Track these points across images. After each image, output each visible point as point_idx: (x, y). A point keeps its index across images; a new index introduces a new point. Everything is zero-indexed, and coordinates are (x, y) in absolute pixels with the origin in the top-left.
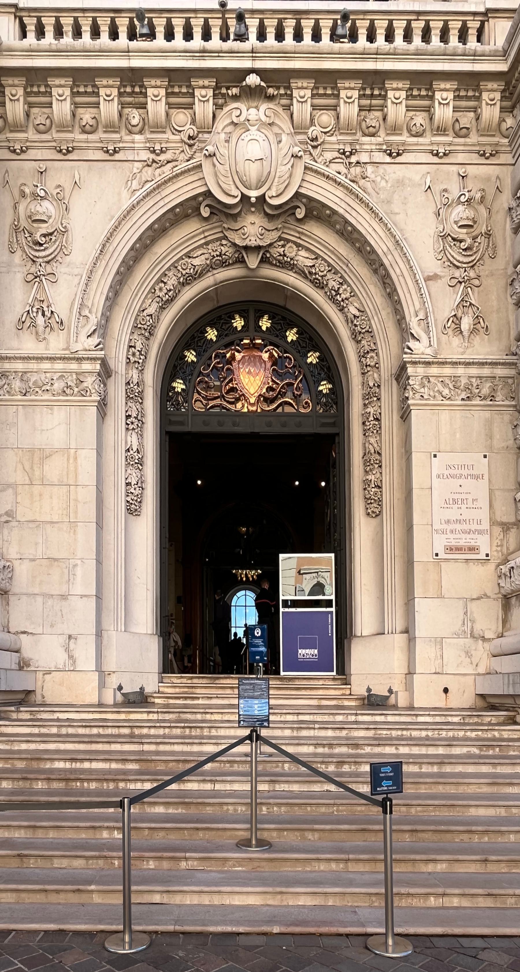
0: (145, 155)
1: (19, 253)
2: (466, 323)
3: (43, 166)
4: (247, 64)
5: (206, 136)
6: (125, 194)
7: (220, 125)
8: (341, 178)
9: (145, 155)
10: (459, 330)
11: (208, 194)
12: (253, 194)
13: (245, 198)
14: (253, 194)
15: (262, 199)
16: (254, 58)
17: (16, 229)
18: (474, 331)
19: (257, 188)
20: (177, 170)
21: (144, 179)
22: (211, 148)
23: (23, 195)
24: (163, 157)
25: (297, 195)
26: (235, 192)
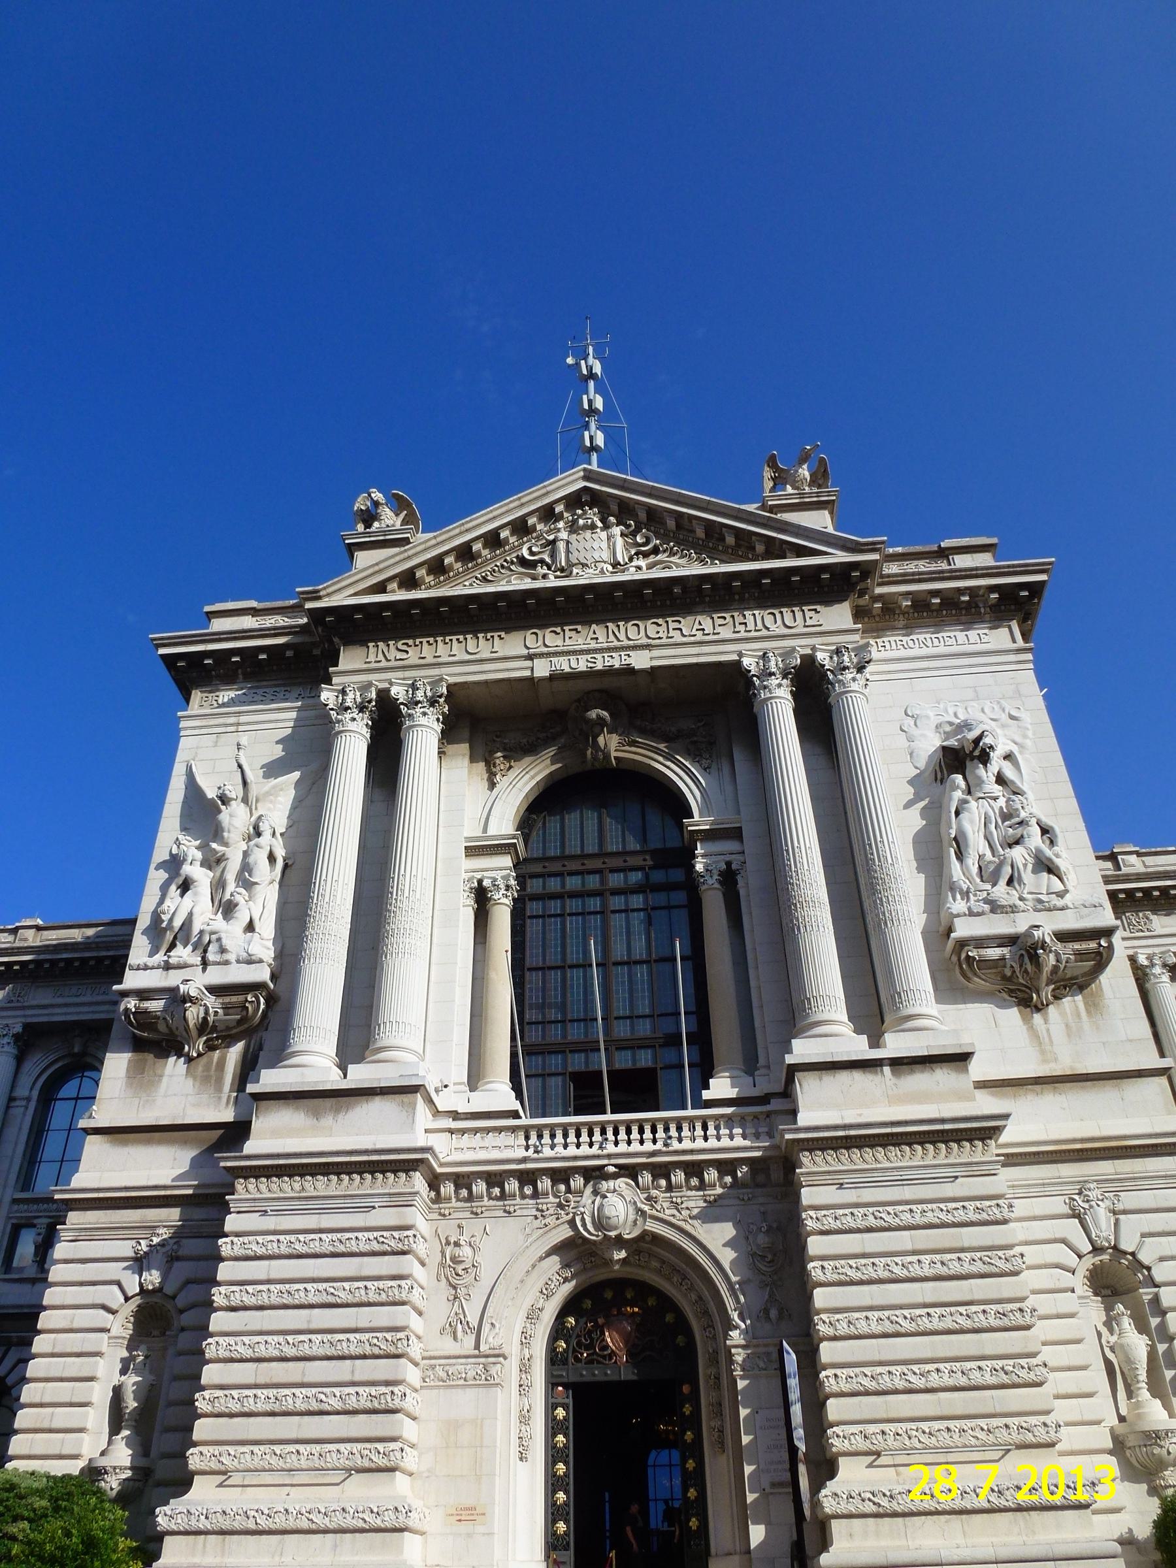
1: (444, 1280)
2: (773, 1313)
4: (605, 1162)
6: (521, 1237)
9: (534, 1212)
10: (768, 1318)
15: (619, 1237)
16: (609, 1159)
17: (442, 1265)
18: (780, 1317)
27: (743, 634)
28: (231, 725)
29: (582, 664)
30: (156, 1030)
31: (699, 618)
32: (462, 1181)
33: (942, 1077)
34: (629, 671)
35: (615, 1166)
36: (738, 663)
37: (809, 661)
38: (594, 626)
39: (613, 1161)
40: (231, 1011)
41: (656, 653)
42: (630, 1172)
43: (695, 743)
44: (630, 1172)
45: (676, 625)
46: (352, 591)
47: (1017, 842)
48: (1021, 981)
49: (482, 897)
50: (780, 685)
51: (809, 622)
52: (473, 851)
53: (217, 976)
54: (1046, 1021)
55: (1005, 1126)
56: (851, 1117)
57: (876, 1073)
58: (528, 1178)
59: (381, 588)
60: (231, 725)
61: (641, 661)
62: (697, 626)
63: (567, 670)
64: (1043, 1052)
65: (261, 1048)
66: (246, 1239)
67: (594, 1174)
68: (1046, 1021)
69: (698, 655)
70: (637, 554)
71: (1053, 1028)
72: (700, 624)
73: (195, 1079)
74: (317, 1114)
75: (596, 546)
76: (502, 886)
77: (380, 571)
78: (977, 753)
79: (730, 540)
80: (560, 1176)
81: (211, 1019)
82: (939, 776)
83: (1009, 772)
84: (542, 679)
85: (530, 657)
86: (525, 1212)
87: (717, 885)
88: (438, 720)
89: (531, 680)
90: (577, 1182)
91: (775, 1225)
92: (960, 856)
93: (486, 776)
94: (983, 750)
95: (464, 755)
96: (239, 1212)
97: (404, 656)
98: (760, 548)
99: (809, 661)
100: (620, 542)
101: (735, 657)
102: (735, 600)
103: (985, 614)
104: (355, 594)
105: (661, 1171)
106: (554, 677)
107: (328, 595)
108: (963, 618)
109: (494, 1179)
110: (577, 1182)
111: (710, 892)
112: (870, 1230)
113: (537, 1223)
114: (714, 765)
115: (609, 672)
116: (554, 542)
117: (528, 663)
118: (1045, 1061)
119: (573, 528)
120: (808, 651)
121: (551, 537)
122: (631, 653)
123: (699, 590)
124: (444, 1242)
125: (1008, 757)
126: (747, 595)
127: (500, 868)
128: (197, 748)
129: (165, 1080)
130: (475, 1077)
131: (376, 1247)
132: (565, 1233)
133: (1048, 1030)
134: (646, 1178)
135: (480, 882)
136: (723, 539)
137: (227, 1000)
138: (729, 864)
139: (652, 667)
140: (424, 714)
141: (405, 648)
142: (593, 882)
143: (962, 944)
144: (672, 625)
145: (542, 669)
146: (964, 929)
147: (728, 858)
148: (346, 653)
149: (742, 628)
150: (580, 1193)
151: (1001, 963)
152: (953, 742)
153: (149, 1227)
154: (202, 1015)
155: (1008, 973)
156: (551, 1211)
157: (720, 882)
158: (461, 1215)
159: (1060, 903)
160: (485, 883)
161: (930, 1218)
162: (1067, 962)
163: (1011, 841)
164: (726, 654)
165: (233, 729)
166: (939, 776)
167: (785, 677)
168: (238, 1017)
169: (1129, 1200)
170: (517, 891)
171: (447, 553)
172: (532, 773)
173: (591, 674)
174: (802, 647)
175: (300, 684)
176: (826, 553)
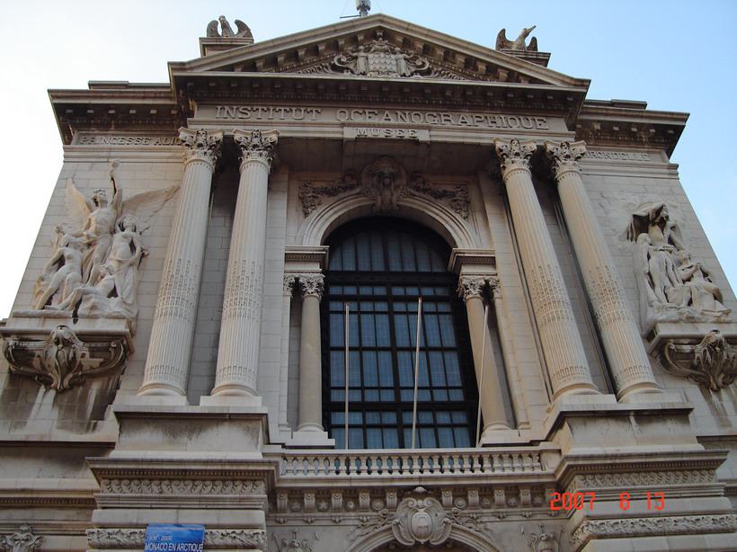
0: (357, 522)
3: (297, 529)
5: (393, 513)
7: (400, 508)
8: (472, 531)
9: (357, 522)
11: (396, 540)
12: (422, 541)
13: (418, 544)
14: (422, 541)
19: (424, 538)
20: (377, 531)
21: (357, 534)
22: (397, 520)
23: (285, 545)
24: (368, 524)
25: (449, 539)
26: (412, 540)
27: (494, 128)
28: (104, 157)
29: (381, 134)
30: (31, 366)
31: (462, 115)
32: (297, 494)
33: (670, 428)
34: (415, 142)
36: (493, 146)
37: (541, 150)
38: (387, 112)
39: (422, 483)
40: (97, 354)
41: (433, 133)
42: (434, 492)
43: (455, 201)
44: (434, 492)
45: (447, 118)
46: (209, 68)
47: (689, 280)
48: (703, 369)
49: (297, 289)
51: (539, 127)
52: (290, 258)
53: (83, 326)
54: (720, 399)
55: (725, 460)
56: (611, 450)
57: (625, 421)
58: (351, 494)
59: (231, 68)
60: (104, 157)
61: (423, 136)
62: (461, 120)
63: (370, 136)
64: (721, 420)
65: (118, 388)
66: (110, 530)
67: (404, 492)
68: (720, 399)
69: (463, 137)
70: (416, 72)
71: (724, 403)
72: (463, 118)
73: (61, 407)
74: (174, 434)
75: (388, 62)
76: (315, 284)
78: (657, 221)
79: (482, 67)
80: (378, 493)
81: (79, 359)
82: (630, 236)
83: (676, 239)
84: (349, 141)
85: (343, 125)
86: (348, 522)
87: (478, 296)
89: (341, 141)
90: (392, 499)
91: (551, 536)
92: (652, 285)
93: (301, 208)
94: (662, 218)
95: (284, 192)
96: (104, 508)
97: (245, 116)
98: (503, 74)
99: (541, 150)
100: (403, 63)
101: (491, 142)
102: (487, 107)
105: (460, 491)
106: (358, 140)
107: (192, 69)
109: (323, 494)
110: (392, 499)
111: (474, 300)
112: (636, 535)
113: (358, 532)
114: (470, 216)
116: (356, 58)
117: (339, 129)
118: (724, 426)
119: (368, 50)
120: (542, 144)
121: (355, 54)
123: (464, 95)
124: (279, 543)
125: (673, 228)
127: (312, 273)
128: (76, 170)
129: (35, 408)
130: (295, 422)
131: (229, 541)
132: (383, 540)
133: (722, 405)
134: (447, 498)
135: (297, 279)
136: (476, 69)
137: (93, 345)
138: (487, 282)
139: (431, 142)
140: (261, 155)
141: (246, 111)
142: (380, 291)
143: (664, 340)
144: (443, 118)
145: (350, 133)
146: (663, 331)
147: (487, 278)
148: (200, 111)
149: (494, 125)
150: (394, 508)
151: (692, 356)
152: (642, 212)
153: (15, 524)
154: (71, 355)
155: (695, 362)
156: (371, 523)
157: (481, 294)
158: (294, 523)
159: (728, 319)
160: (301, 281)
161: (681, 526)
163: (685, 278)
164: (486, 139)
165: (105, 160)
166: (630, 236)
167: (526, 157)
168: (102, 360)
171: (280, 53)
172: (335, 209)
173: (386, 140)
174: (541, 141)
175: (158, 135)
176: (550, 84)
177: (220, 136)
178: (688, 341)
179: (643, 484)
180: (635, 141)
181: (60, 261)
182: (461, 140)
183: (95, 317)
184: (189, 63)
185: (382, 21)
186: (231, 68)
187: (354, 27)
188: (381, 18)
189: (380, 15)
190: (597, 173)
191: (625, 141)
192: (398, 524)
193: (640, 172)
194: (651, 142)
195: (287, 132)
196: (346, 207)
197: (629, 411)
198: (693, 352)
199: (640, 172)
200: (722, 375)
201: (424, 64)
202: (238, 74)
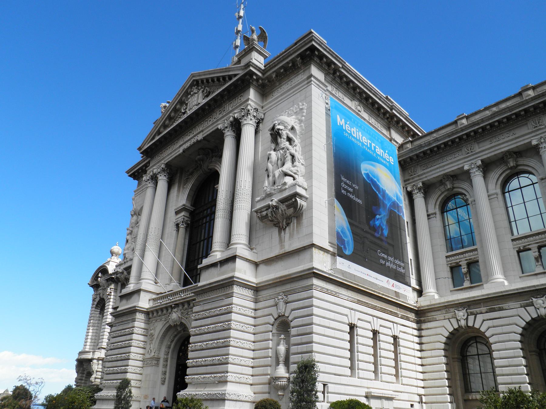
34: (198, 142)
35: (174, 304)
42: (177, 305)
46: (147, 143)
49: (177, 225)
50: (228, 131)
61: (200, 137)
63: (186, 147)
68: (285, 234)
77: (152, 134)
88: (165, 176)
103: (301, 66)
104: (148, 144)
106: (184, 151)
107: (143, 147)
108: (295, 72)
115: (194, 144)
122: (198, 135)
126: (224, 100)
133: (284, 237)
145: (181, 150)
162: (285, 210)
169: (291, 297)
170: (190, 221)
173: (191, 146)
177: (163, 166)
178: (265, 209)
179: (212, 296)
180: (295, 69)
181: (127, 241)
182: (211, 131)
183: (127, 262)
184: (141, 146)
185: (193, 77)
186: (153, 138)
187: (185, 88)
188: (192, 75)
189: (192, 74)
190: (268, 110)
191: (290, 73)
192: (170, 319)
193: (293, 92)
194: (303, 64)
195: (168, 159)
196: (194, 178)
197: (217, 262)
198: (267, 214)
199: (293, 92)
200: (285, 221)
201: (207, 90)
202: (157, 138)
